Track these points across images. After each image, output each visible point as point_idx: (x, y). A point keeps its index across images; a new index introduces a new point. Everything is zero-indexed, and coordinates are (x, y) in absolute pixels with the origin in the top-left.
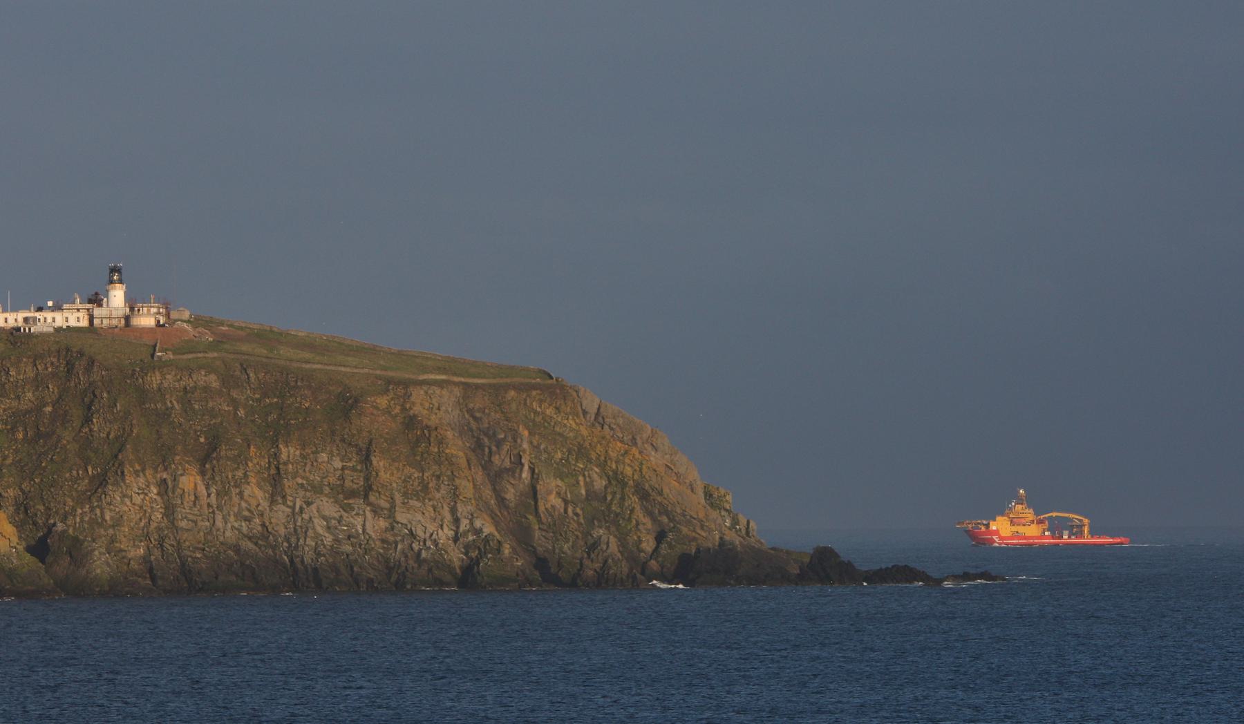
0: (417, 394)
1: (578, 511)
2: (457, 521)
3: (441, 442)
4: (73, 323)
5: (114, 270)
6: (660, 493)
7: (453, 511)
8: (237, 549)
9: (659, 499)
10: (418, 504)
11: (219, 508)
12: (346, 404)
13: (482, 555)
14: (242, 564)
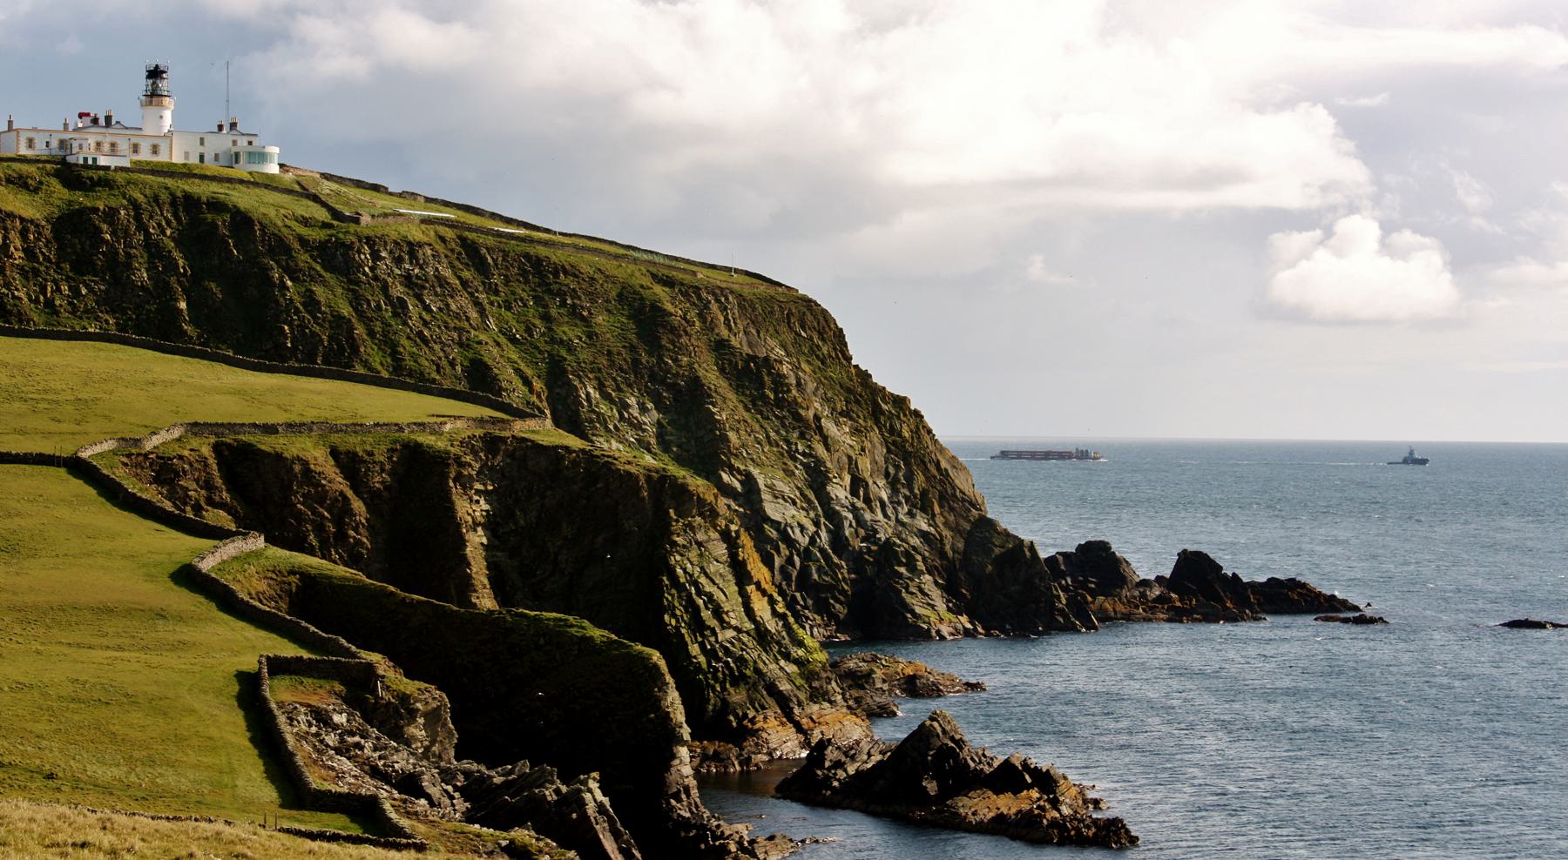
5: (155, 74)
6: (938, 464)
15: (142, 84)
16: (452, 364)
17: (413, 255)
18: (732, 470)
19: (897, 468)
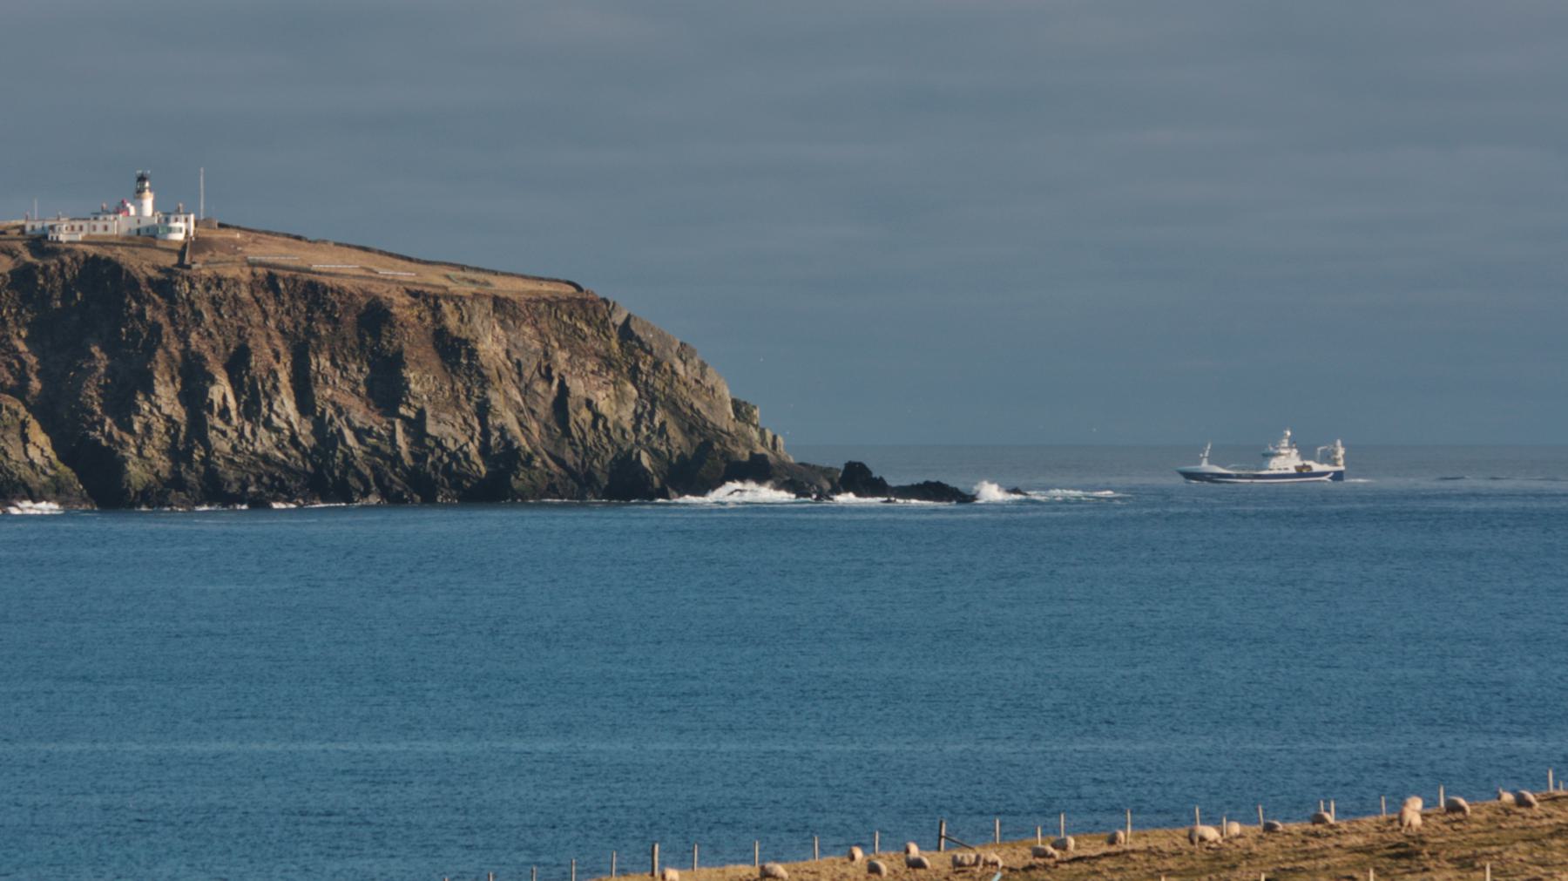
0: (447, 307)
1: (610, 425)
2: (486, 433)
3: (472, 354)
4: (100, 231)
6: (691, 407)
7: (483, 423)
8: (265, 458)
9: (689, 412)
10: (447, 417)
11: (249, 419)
12: (375, 316)
13: (512, 468)
14: (272, 476)
15: (134, 185)
16: (227, 348)
17: (219, 286)
18: (409, 405)
19: (644, 407)
